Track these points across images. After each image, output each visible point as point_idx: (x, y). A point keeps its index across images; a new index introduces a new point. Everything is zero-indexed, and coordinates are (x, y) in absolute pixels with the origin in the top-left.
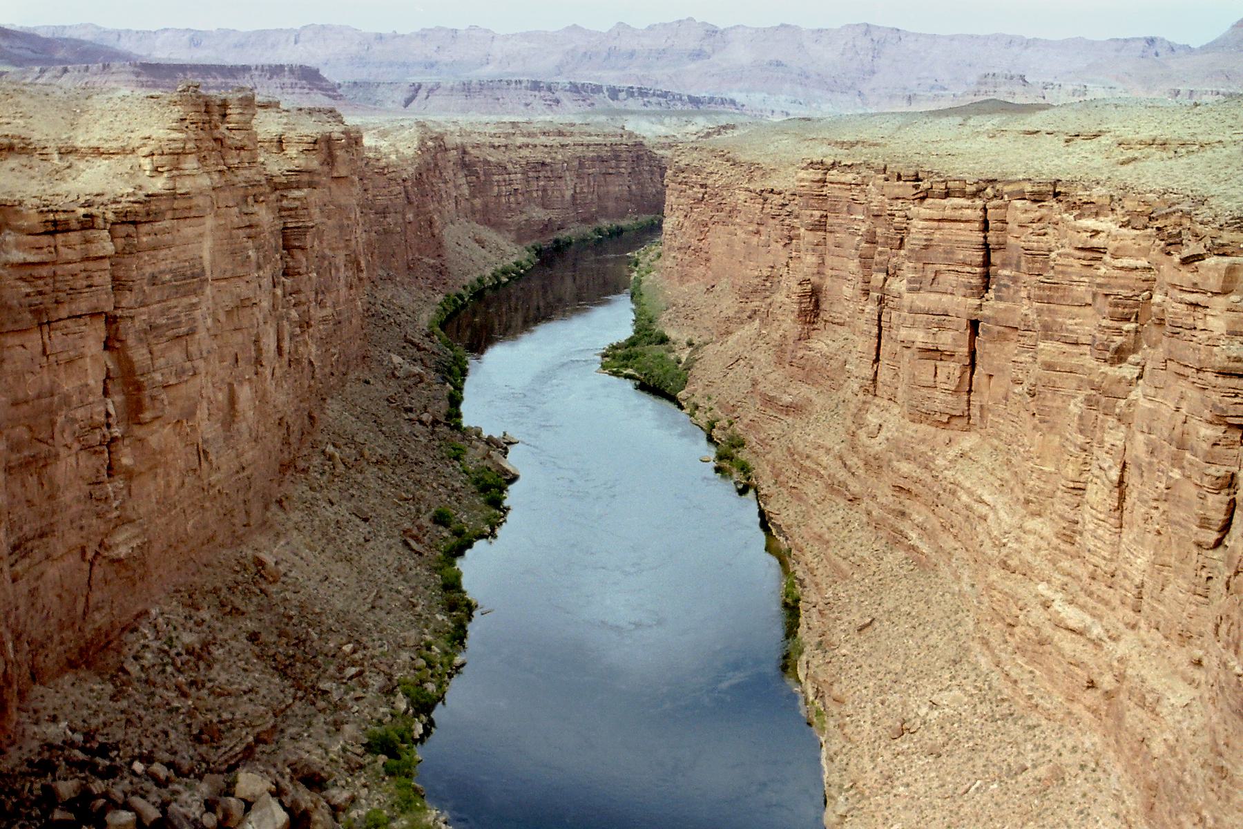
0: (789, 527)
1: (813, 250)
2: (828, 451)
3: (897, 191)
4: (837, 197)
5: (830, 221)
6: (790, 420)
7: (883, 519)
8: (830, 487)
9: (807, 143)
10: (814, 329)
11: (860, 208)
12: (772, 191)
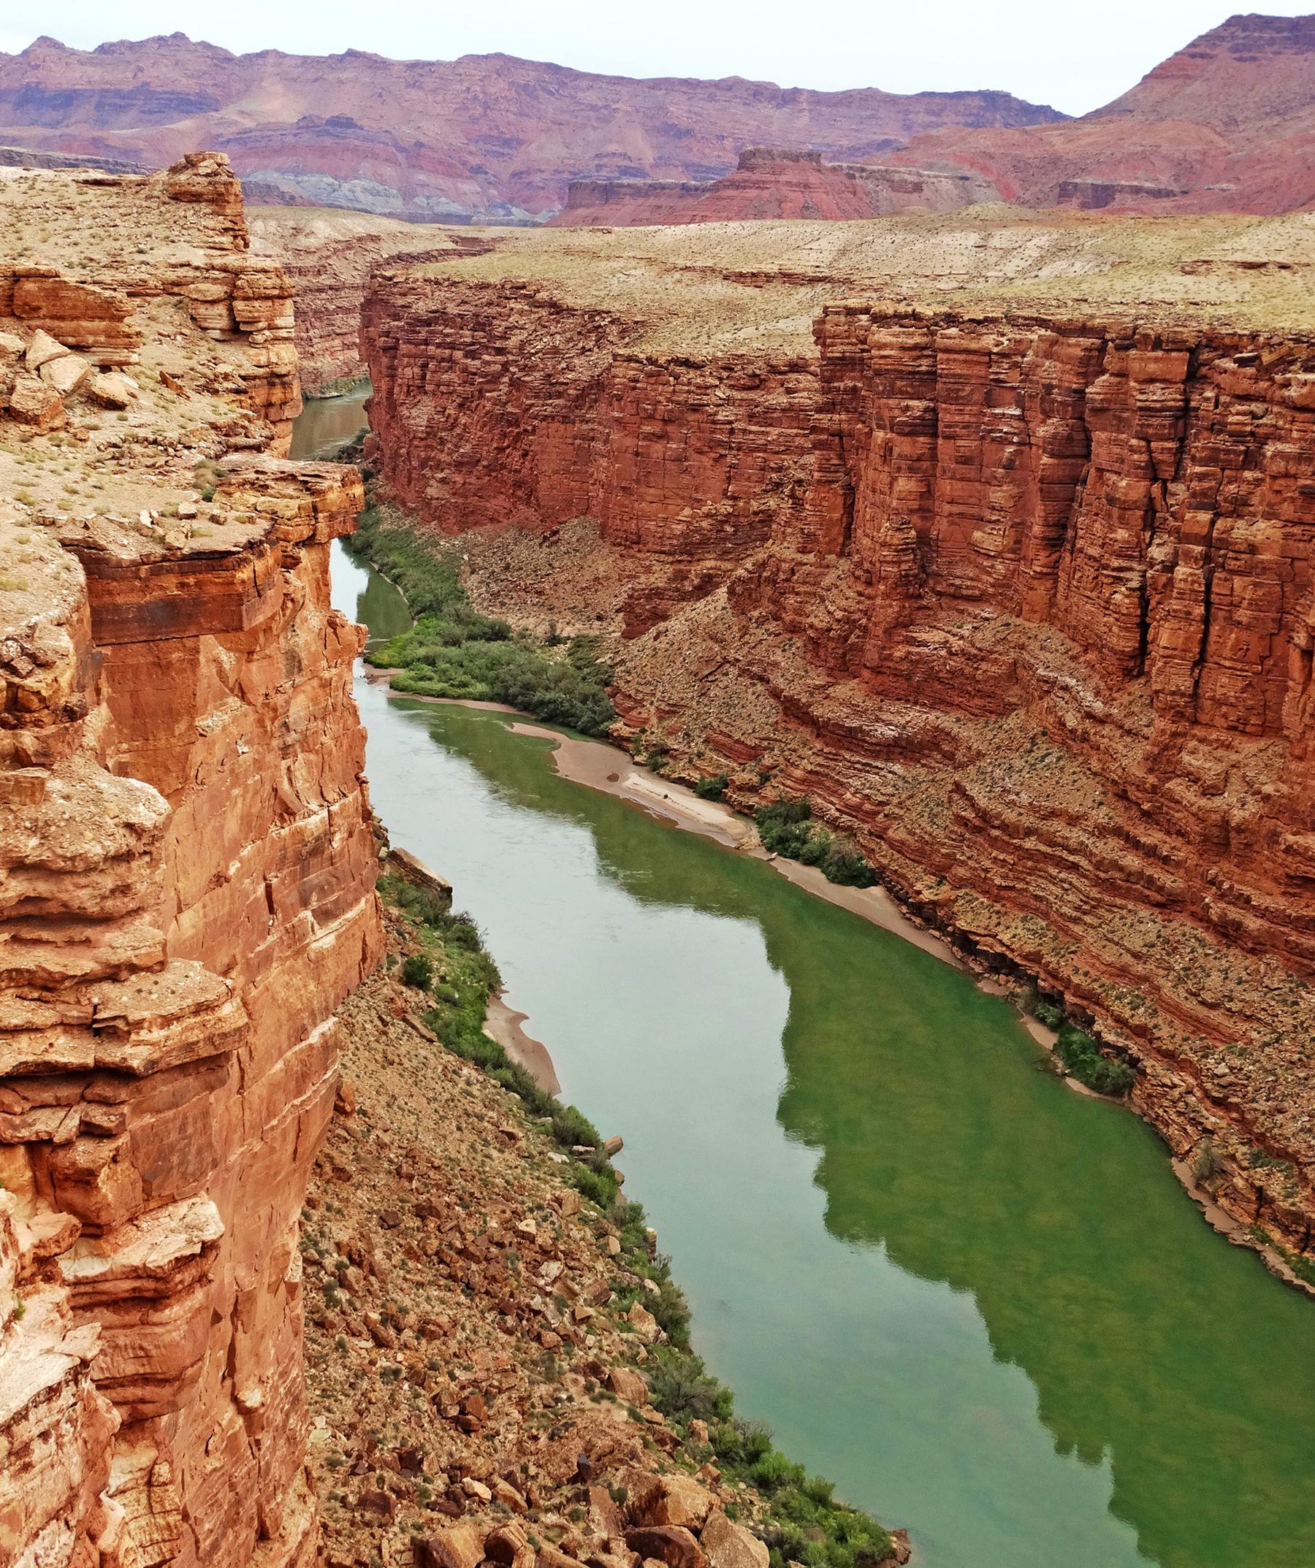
0: (1036, 957)
1: (911, 469)
2: (1073, 820)
3: (1152, 367)
4: (960, 376)
5: (945, 418)
6: (897, 768)
7: (1273, 935)
8: (1110, 886)
9: (677, 276)
10: (919, 608)
11: (1009, 396)
12: (687, 363)
